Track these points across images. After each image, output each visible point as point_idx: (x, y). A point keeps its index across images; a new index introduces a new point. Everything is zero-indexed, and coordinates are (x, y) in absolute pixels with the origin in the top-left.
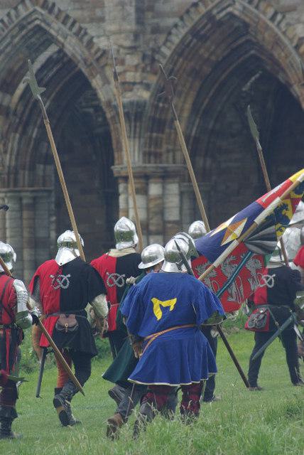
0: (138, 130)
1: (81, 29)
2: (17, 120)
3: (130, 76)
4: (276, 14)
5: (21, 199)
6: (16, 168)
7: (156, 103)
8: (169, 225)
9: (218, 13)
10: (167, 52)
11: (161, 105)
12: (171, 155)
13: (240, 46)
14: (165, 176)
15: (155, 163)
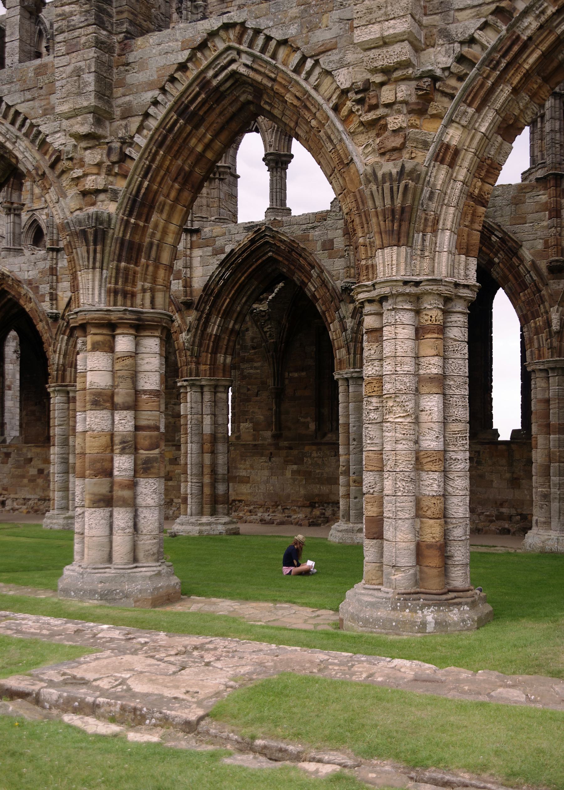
0: (99, 256)
1: (32, 126)
2: (65, 324)
3: (90, 183)
4: (304, 59)
5: (68, 393)
6: (63, 365)
7: (125, 218)
8: (144, 397)
9: (216, 76)
10: (141, 141)
11: (132, 221)
12: (148, 295)
13: (258, 248)
14: (139, 327)
15: (124, 305)
